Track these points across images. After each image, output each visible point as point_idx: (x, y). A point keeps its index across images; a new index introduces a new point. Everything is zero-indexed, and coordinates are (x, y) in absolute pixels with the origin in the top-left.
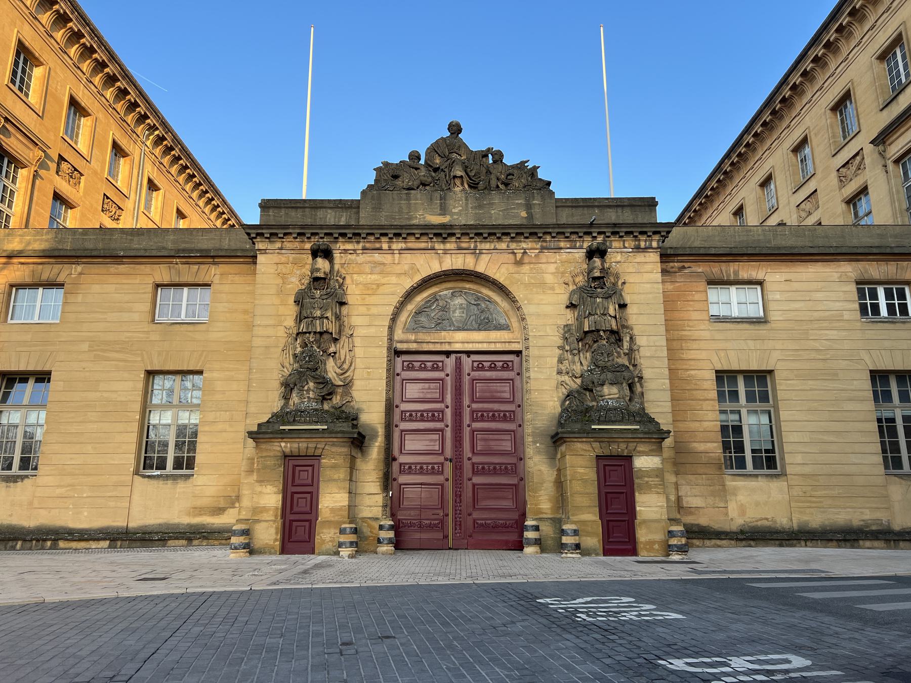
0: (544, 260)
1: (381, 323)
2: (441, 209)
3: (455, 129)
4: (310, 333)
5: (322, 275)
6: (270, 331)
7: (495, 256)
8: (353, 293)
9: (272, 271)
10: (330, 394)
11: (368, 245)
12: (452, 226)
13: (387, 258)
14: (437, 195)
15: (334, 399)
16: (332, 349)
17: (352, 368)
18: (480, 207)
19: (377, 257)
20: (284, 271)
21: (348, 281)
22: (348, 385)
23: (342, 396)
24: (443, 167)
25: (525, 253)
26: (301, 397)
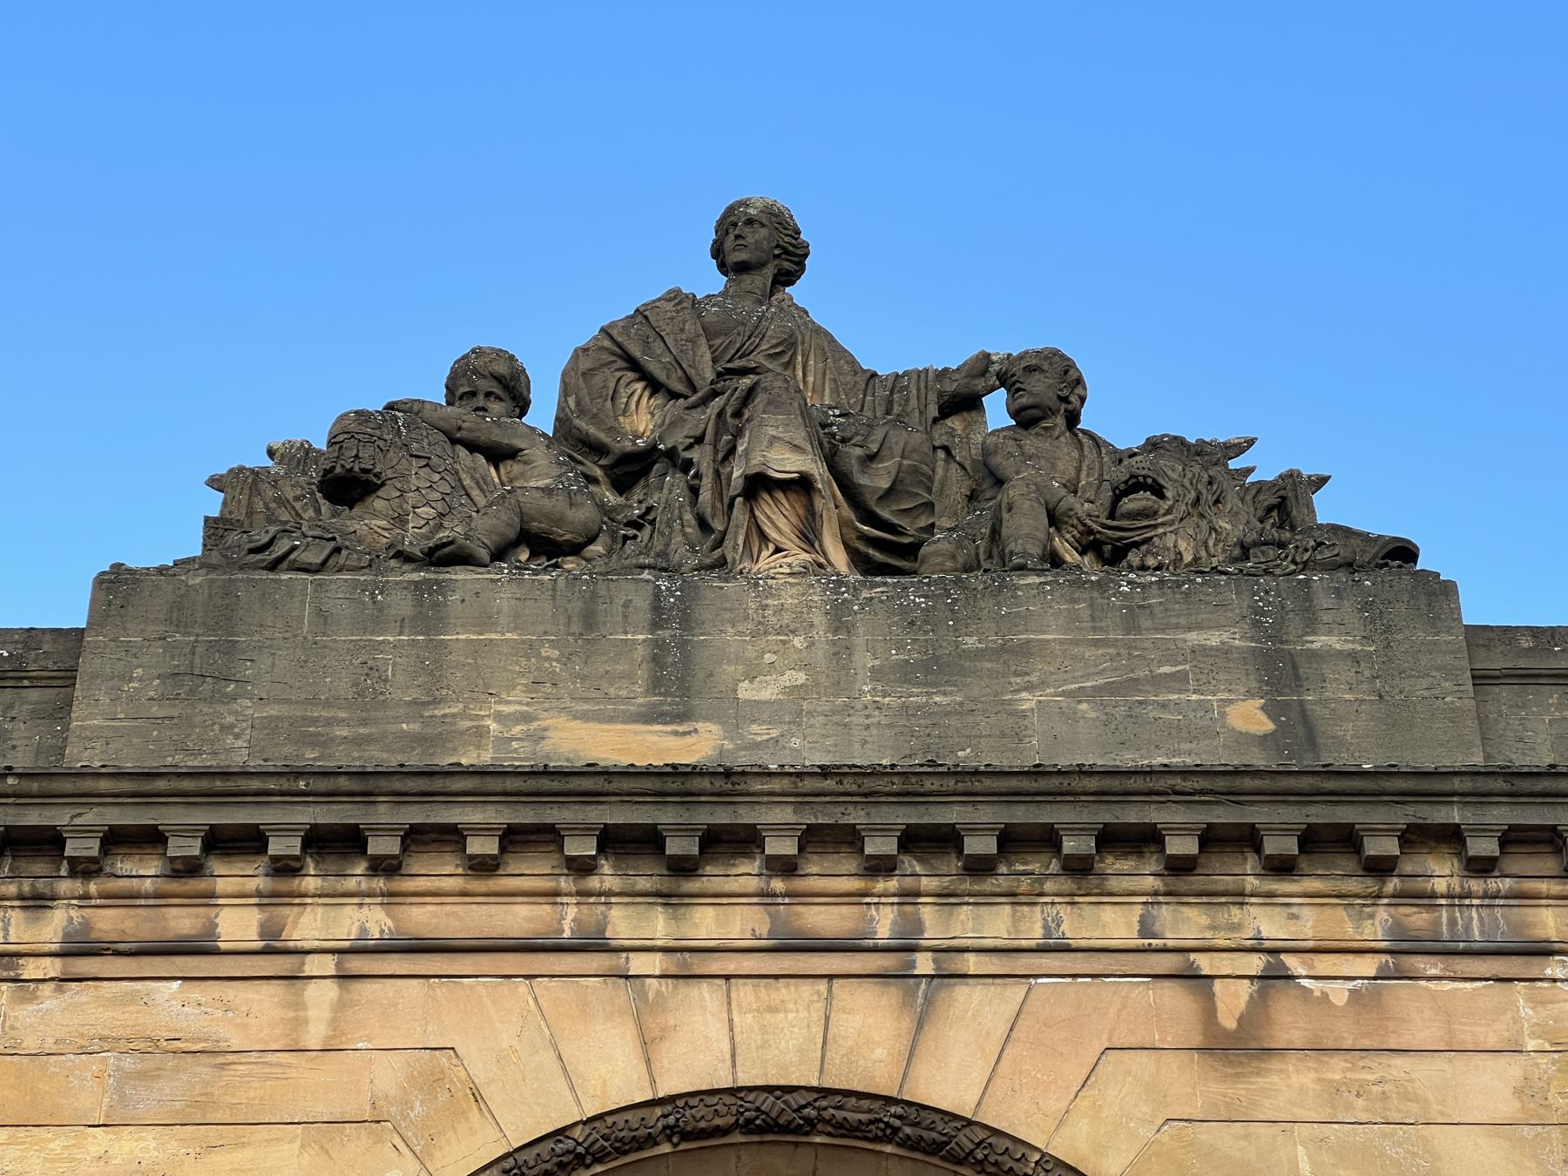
0: (1424, 1032)
2: (656, 684)
3: (762, 250)
7: (1054, 996)
11: (109, 922)
12: (727, 780)
13: (253, 1012)
14: (635, 593)
18: (934, 669)
19: (172, 1003)
24: (678, 439)
25: (1275, 977)
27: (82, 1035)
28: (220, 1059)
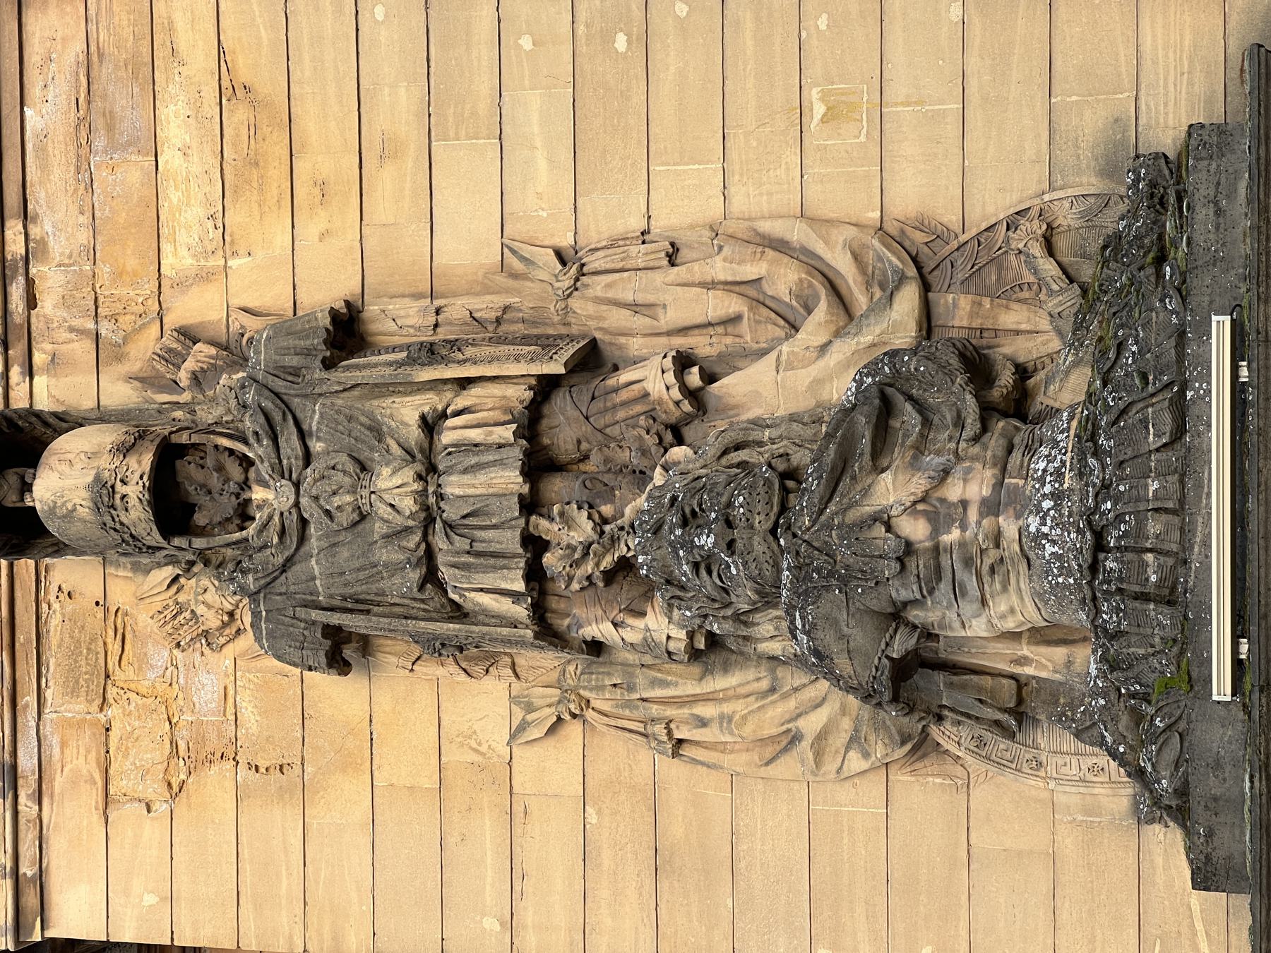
1: (484, 53)
4: (535, 545)
5: (142, 463)
6: (550, 845)
8: (275, 272)
9: (152, 831)
10: (977, 366)
15: (1023, 349)
16: (654, 380)
17: (797, 233)
20: (154, 754)
21: (200, 306)
22: (924, 261)
23: (1008, 293)
26: (987, 565)
27: (75, 190)
28: (95, 58)
